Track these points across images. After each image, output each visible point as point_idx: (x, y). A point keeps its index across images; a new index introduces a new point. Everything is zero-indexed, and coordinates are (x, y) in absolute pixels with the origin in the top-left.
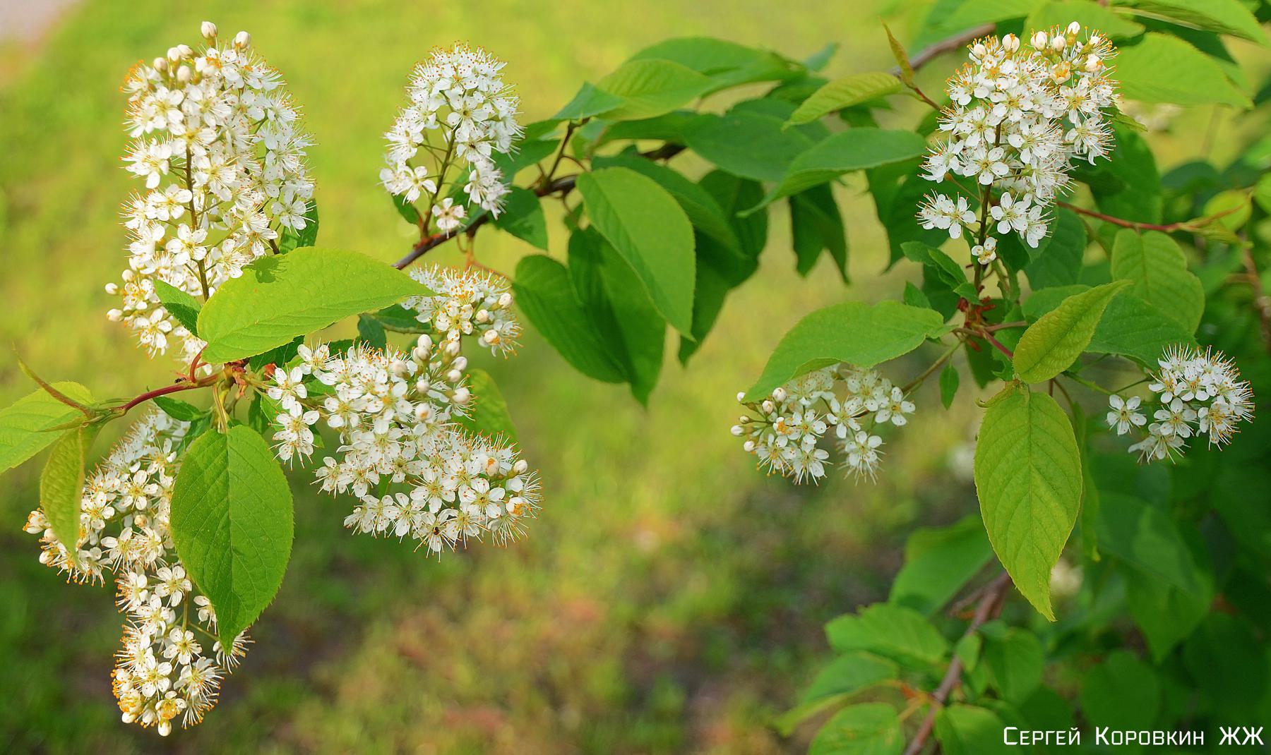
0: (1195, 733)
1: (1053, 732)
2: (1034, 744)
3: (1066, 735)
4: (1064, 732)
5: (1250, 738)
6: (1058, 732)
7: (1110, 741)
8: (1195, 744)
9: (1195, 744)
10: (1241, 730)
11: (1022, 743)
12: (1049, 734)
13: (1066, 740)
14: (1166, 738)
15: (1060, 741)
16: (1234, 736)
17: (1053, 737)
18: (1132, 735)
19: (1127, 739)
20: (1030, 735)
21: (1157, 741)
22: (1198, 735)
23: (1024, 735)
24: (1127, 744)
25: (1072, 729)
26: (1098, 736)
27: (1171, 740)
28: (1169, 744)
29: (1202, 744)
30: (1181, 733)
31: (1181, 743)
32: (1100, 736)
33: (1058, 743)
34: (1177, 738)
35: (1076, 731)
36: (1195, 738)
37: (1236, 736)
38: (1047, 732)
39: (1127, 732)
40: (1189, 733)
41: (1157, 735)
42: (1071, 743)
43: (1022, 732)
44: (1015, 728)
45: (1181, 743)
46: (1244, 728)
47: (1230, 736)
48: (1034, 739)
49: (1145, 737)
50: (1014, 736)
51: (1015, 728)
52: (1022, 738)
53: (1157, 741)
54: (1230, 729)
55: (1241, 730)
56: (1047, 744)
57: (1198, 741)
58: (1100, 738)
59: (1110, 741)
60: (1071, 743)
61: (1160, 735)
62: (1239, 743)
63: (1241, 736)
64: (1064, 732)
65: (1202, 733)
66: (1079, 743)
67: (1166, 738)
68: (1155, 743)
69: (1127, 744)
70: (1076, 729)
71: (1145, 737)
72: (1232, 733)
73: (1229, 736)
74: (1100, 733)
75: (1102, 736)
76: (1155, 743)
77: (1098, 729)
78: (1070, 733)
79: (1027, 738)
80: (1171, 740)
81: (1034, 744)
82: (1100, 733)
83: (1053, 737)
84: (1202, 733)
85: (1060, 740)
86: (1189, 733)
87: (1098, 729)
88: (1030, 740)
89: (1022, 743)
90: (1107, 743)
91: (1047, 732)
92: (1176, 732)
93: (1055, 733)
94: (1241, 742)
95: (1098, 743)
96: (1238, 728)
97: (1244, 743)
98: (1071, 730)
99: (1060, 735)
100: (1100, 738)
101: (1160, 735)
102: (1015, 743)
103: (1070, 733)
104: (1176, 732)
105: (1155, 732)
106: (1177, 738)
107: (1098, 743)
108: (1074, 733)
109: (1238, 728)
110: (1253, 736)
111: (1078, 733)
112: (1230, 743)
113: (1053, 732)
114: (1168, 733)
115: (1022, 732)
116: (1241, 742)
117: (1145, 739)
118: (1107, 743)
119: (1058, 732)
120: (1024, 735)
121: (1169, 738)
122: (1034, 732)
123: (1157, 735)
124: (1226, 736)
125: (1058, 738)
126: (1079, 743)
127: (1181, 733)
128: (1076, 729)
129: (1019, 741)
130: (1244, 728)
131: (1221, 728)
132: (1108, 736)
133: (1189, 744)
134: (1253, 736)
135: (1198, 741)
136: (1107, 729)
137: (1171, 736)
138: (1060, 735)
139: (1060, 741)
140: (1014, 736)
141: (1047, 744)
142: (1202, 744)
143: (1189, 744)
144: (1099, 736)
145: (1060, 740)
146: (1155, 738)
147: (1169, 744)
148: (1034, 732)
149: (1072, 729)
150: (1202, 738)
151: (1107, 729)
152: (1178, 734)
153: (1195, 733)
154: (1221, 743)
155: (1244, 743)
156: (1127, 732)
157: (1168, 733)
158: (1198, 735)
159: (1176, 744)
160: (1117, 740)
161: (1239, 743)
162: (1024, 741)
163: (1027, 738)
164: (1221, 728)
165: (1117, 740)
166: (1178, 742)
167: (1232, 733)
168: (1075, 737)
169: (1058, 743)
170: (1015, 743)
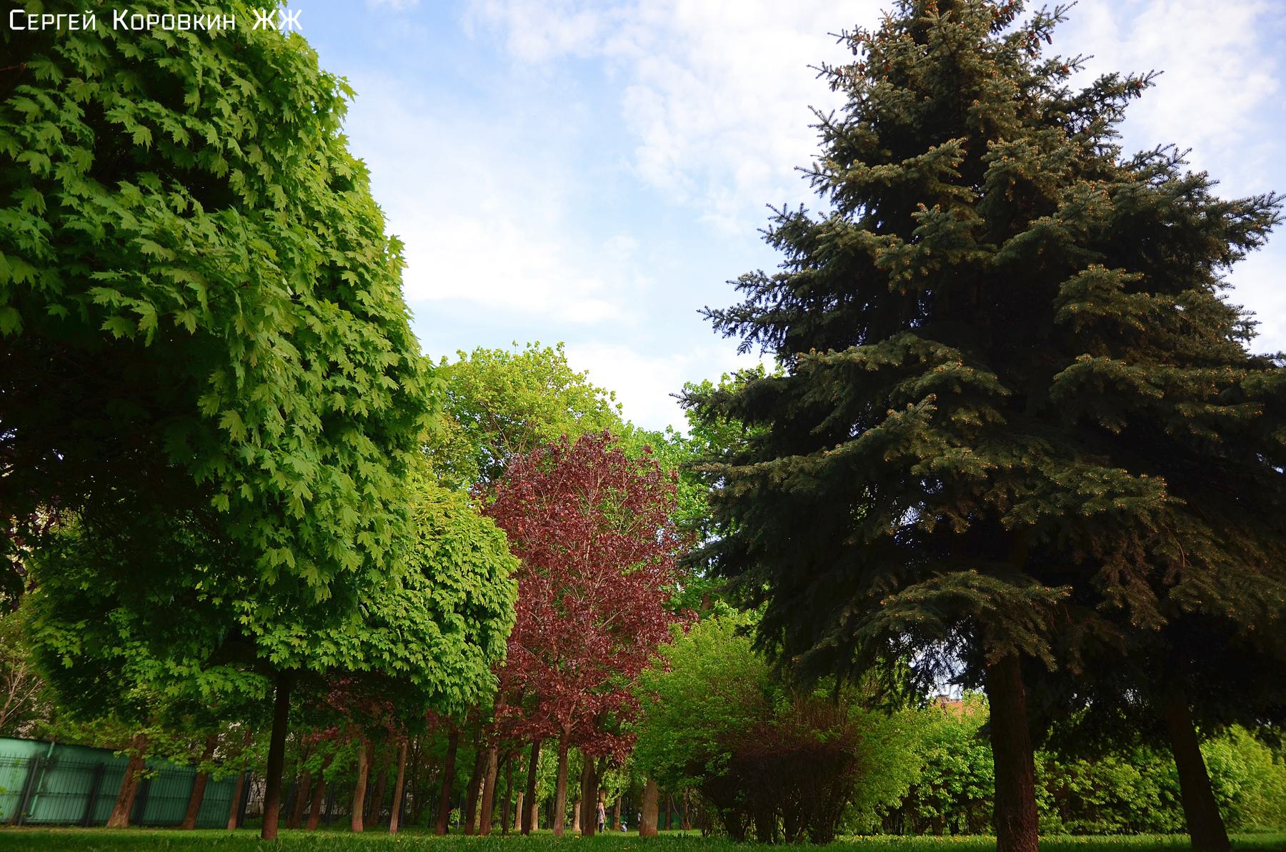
3: (80, 19)
7: (128, 25)
11: (30, 28)
13: (81, 24)
15: (74, 25)
19: (149, 23)
20: (40, 19)
21: (183, 25)
23: (33, 19)
26: (116, 19)
33: (71, 28)
38: (59, 16)
41: (183, 18)
43: (30, 16)
44: (22, 11)
48: (44, 23)
50: (20, 20)
53: (183, 25)
58: (118, 23)
60: (85, 28)
75: (121, 19)
76: (180, 28)
77: (115, 12)
88: (39, 25)
89: (30, 28)
90: (126, 28)
91: (59, 16)
100: (118, 23)
102: (22, 28)
105: (180, 16)
108: (88, 17)
111: (93, 17)
118: (126, 28)
119: (71, 16)
120: (33, 19)
121: (196, 22)
122: (44, 16)
125: (71, 22)
132: (127, 20)
137: (198, 19)
138: (74, 18)
139: (74, 25)
146: (180, 22)
148: (44, 16)
151: (126, 11)
162: (33, 25)
165: (137, 23)
170: (22, 28)
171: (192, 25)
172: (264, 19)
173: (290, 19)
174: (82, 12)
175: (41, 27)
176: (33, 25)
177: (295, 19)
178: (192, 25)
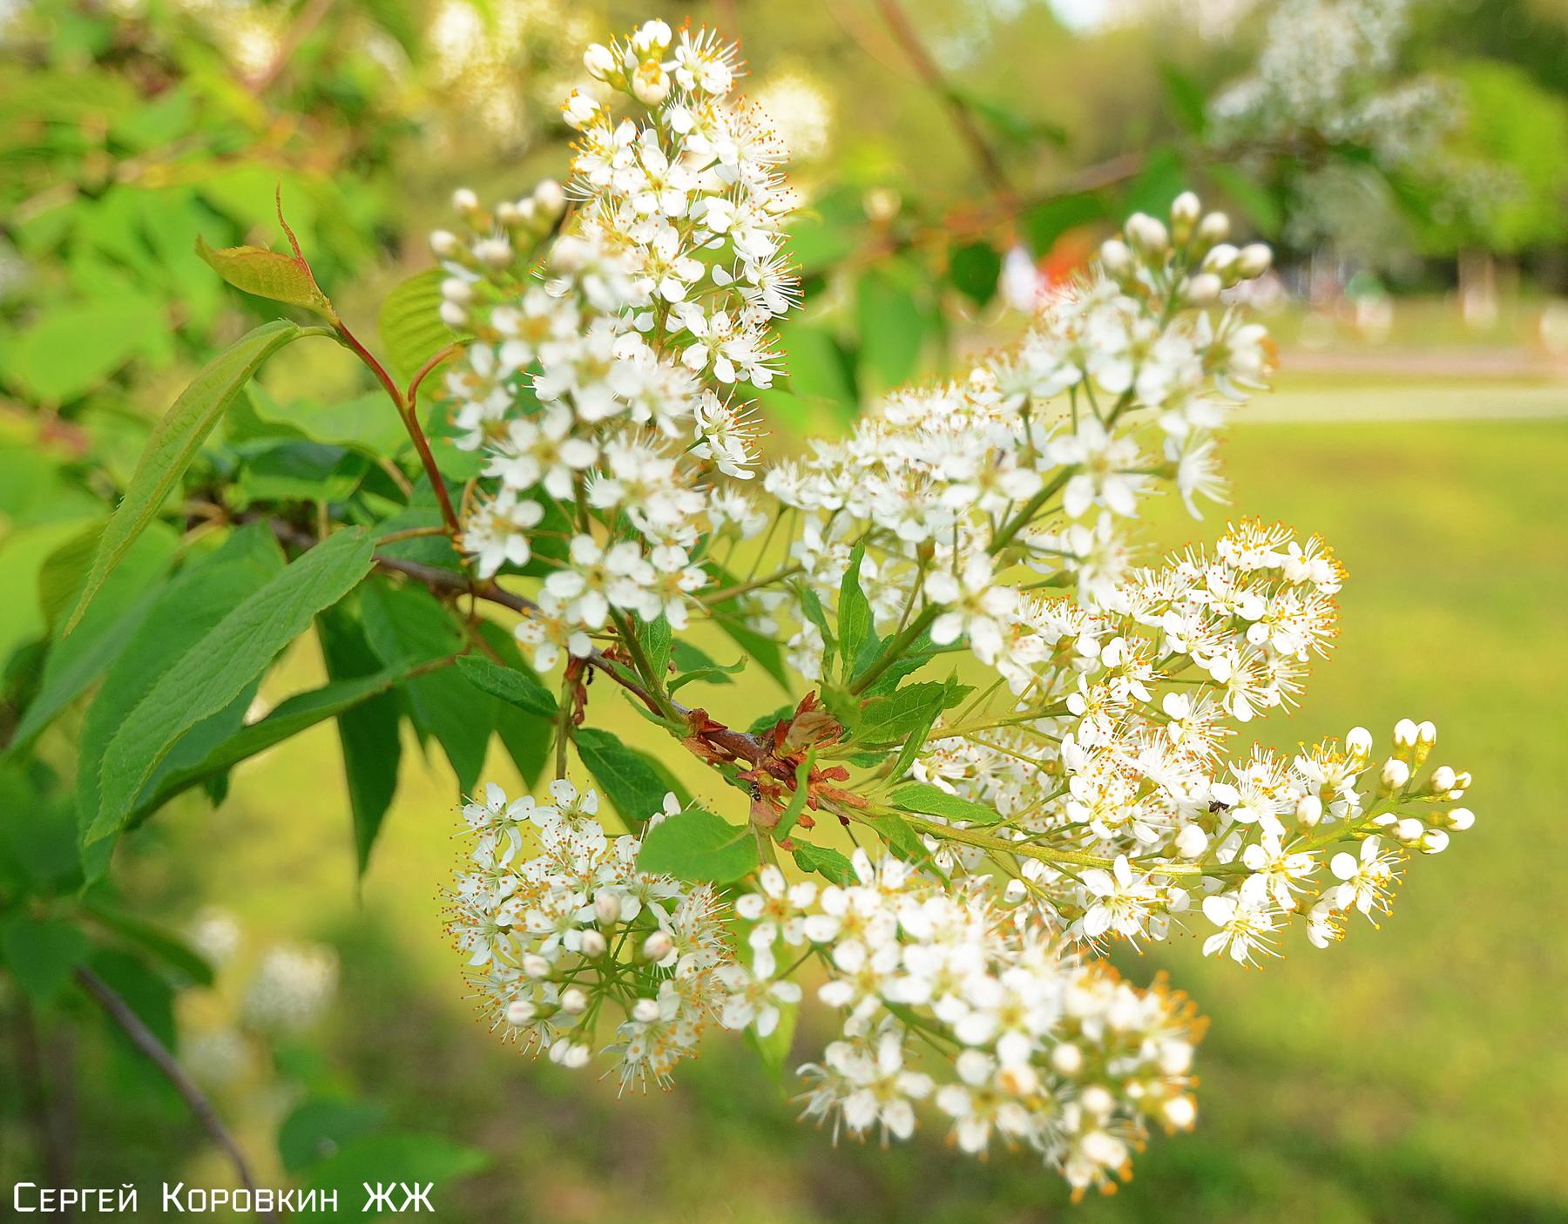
0: (323, 1192)
1: (94, 1191)
2: (62, 1210)
3: (115, 1196)
4: (111, 1191)
5: (413, 1201)
6: (101, 1192)
7: (185, 1205)
8: (323, 1209)
9: (323, 1209)
10: (398, 1188)
11: (43, 1209)
12: (65, 1194)
13: (115, 1204)
14: (276, 1201)
15: (106, 1205)
17: (93, 1199)
18: (220, 1197)
19: (214, 1202)
20: (56, 1196)
21: (263, 1205)
22: (329, 1195)
23: (47, 1195)
24: (213, 1210)
25: (124, 1185)
26: (166, 1197)
27: (284, 1204)
28: (280, 1210)
29: (335, 1209)
30: (300, 1192)
34: (294, 1200)
35: (130, 1190)
36: (323, 1200)
38: (84, 1191)
40: (313, 1193)
41: (262, 1196)
42: (122, 1208)
43: (43, 1192)
44: (32, 1185)
45: (301, 1208)
47: (380, 1197)
48: (63, 1202)
49: (242, 1204)
50: (29, 1197)
51: (32, 1185)
52: (43, 1200)
54: (380, 1186)
55: (398, 1188)
56: (84, 1209)
57: (329, 1205)
58: (170, 1201)
59: (185, 1205)
60: (122, 1208)
61: (267, 1195)
62: (394, 1209)
63: (398, 1197)
64: (111, 1191)
65: (335, 1192)
66: (135, 1209)
67: (276, 1201)
68: (258, 1209)
69: (213, 1210)
70: (131, 1185)
71: (242, 1197)
72: (383, 1193)
73: (379, 1196)
74: (170, 1192)
75: (173, 1197)
76: (258, 1209)
77: (165, 1186)
78: (121, 1192)
79: (51, 1200)
80: (284, 1204)
81: (62, 1210)
82: (170, 1192)
83: (93, 1199)
84: (335, 1192)
85: (45, 1203)
86: (313, 1193)
87: (165, 1186)
88: (56, 1204)
89: (43, 1209)
90: (181, 1209)
91: (84, 1191)
92: (292, 1191)
93: (97, 1193)
94: (398, 1208)
95: (165, 1209)
96: (393, 1185)
97: (403, 1209)
99: (105, 1195)
100: (170, 1201)
101: (267, 1195)
102: (32, 1209)
103: (121, 1192)
104: (292, 1191)
106: (294, 1200)
107: (165, 1209)
109: (393, 1185)
110: (418, 1197)
111: (134, 1193)
113: (94, 1191)
114: (280, 1192)
115: (43, 1192)
116: (398, 1208)
118: (181, 1209)
119: (101, 1192)
120: (47, 1195)
121: (281, 1201)
122: (63, 1192)
123: (262, 1196)
124: (373, 1197)
125: (102, 1200)
126: (135, 1209)
127: (300, 1192)
128: (131, 1185)
129: (39, 1207)
131: (366, 1185)
132: (182, 1197)
133: (314, 1209)
135: (329, 1205)
136: (180, 1185)
137: (284, 1197)
138: (105, 1195)
139: (106, 1205)
140: (29, 1197)
141: (84, 1209)
142: (335, 1209)
143: (314, 1209)
144: (168, 1196)
145: (45, 1203)
146: (258, 1200)
147: (280, 1210)
148: (63, 1192)
149: (124, 1185)
150: (335, 1200)
151: (180, 1185)
152: (295, 1195)
153: (323, 1192)
155: (403, 1209)
156: (213, 1192)
157: (280, 1192)
158: (329, 1195)
159: (292, 1210)
160: (197, 1201)
161: (394, 1209)
162: (47, 1205)
163: (51, 1200)
164: (366, 1185)
166: (296, 1206)
167: (383, 1193)
168: (129, 1199)
170: (32, 1209)
171: (276, 1206)
173: (417, 1197)
174: (117, 1187)
175: (117, 1207)
176: (47, 1205)
177: (423, 1197)
178: (276, 1206)
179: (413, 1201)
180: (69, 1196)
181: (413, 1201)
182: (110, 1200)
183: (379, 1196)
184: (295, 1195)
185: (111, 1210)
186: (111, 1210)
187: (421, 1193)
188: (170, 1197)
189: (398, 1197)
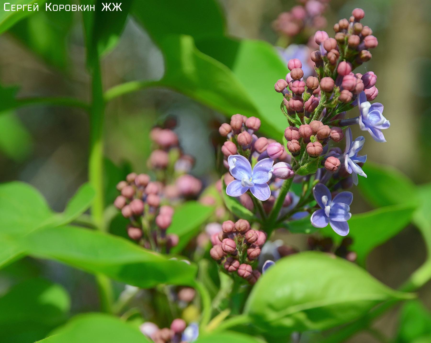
0: (91, 5)
1: (26, 5)
3: (32, 7)
5: (116, 8)
7: (52, 9)
8: (91, 10)
9: (91, 10)
10: (112, 4)
11: (12, 10)
13: (32, 9)
15: (30, 9)
16: (108, 7)
17: (26, 8)
18: (62, 7)
19: (60, 8)
20: (16, 7)
21: (74, 9)
23: (13, 6)
24: (60, 10)
25: (35, 4)
26: (47, 7)
27: (80, 9)
28: (79, 10)
29: (94, 10)
30: (84, 5)
31: (84, 10)
32: (48, 7)
33: (28, 10)
34: (82, 8)
36: (91, 8)
37: (109, 7)
38: (24, 5)
39: (60, 5)
40: (88, 6)
41: (74, 7)
42: (34, 10)
43: (12, 5)
44: (9, 3)
45: (84, 10)
46: (113, 4)
47: (107, 7)
48: (18, 8)
49: (68, 8)
50: (8, 7)
51: (9, 3)
52: (12, 8)
53: (74, 9)
54: (107, 4)
55: (112, 4)
58: (48, 8)
59: (52, 9)
60: (34, 10)
61: (75, 6)
62: (110, 10)
63: (112, 7)
65: (94, 5)
66: (38, 10)
68: (72, 10)
69: (60, 10)
70: (37, 4)
73: (106, 7)
74: (48, 6)
75: (49, 7)
76: (72, 10)
77: (46, 4)
78: (34, 5)
80: (80, 9)
81: (18, 10)
82: (48, 6)
84: (94, 5)
85: (13, 9)
86: (88, 6)
87: (46, 4)
88: (16, 9)
89: (12, 10)
90: (51, 10)
91: (24, 5)
92: (82, 5)
93: (27, 6)
94: (112, 9)
95: (46, 10)
96: (110, 4)
97: (113, 10)
98: (34, 4)
99: (30, 6)
100: (48, 8)
101: (75, 6)
102: (9, 10)
103: (34, 5)
104: (82, 5)
105: (72, 5)
106: (82, 8)
107: (46, 10)
108: (36, 6)
109: (110, 4)
110: (117, 7)
111: (38, 6)
112: (107, 10)
113: (26, 5)
114: (79, 5)
115: (12, 5)
116: (112, 9)
117: (68, 8)
118: (51, 10)
119: (29, 5)
120: (13, 6)
121: (79, 8)
122: (18, 5)
123: (74, 7)
124: (105, 7)
125: (29, 8)
127: (84, 5)
128: (37, 4)
130: (113, 4)
131: (103, 3)
132: (51, 7)
133: (88, 10)
134: (117, 7)
136: (51, 4)
137: (80, 7)
139: (30, 9)
142: (94, 10)
143: (88, 10)
145: (13, 9)
146: (72, 8)
147: (79, 10)
148: (18, 5)
149: (35, 4)
150: (94, 8)
151: (51, 4)
152: (83, 7)
153: (91, 5)
154: (103, 10)
155: (113, 10)
156: (60, 5)
157: (79, 5)
159: (82, 10)
160: (55, 8)
161: (110, 10)
162: (13, 9)
164: (103, 3)
165: (55, 9)
166: (83, 9)
169: (28, 10)
170: (9, 10)
172: (107, 7)
173: (117, 7)
176: (13, 9)
177: (119, 7)
178: (77, 9)
179: (116, 8)
180: (19, 7)
181: (116, 8)
182: (31, 8)
183: (106, 7)
184: (83, 7)
185: (31, 10)
186: (31, 10)
187: (118, 6)
188: (48, 7)
189: (112, 7)
